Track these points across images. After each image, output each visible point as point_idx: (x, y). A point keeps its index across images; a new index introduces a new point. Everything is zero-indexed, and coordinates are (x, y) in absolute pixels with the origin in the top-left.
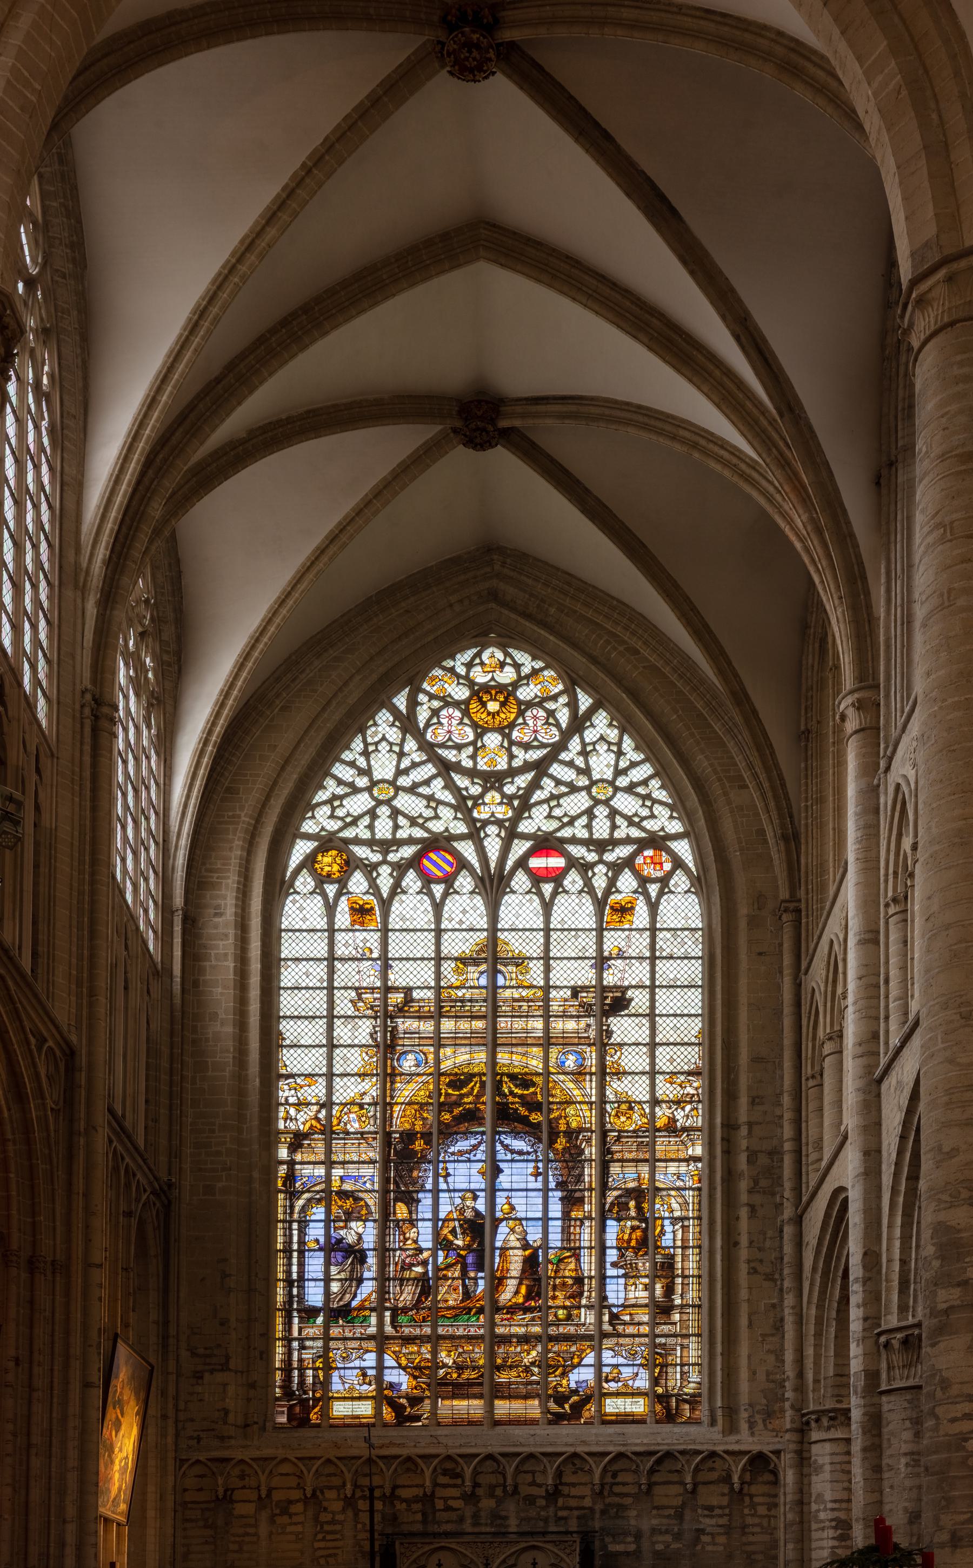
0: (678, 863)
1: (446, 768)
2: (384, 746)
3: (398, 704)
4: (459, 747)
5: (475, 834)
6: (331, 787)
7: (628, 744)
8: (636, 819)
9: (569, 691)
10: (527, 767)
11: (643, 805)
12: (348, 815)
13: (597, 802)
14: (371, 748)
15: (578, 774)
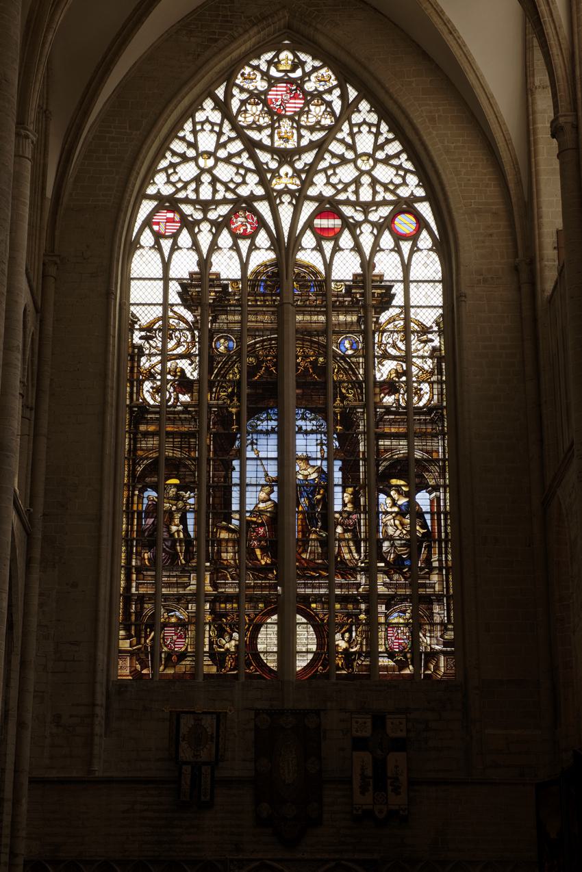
0: (421, 223)
1: (251, 146)
2: (207, 127)
3: (219, 95)
4: (260, 129)
5: (271, 197)
6: (169, 158)
7: (384, 127)
8: (391, 187)
9: (341, 86)
10: (312, 145)
11: (397, 174)
12: (180, 180)
13: (362, 173)
14: (199, 127)
15: (346, 149)
